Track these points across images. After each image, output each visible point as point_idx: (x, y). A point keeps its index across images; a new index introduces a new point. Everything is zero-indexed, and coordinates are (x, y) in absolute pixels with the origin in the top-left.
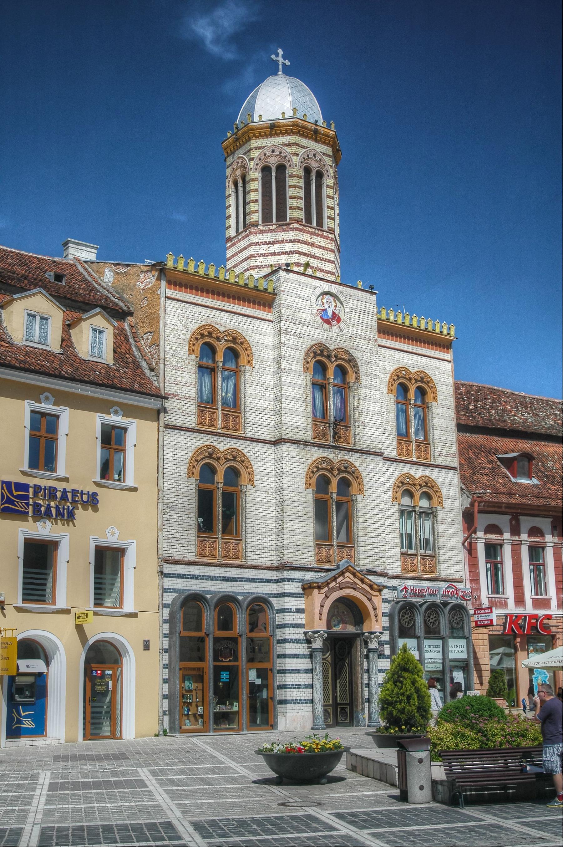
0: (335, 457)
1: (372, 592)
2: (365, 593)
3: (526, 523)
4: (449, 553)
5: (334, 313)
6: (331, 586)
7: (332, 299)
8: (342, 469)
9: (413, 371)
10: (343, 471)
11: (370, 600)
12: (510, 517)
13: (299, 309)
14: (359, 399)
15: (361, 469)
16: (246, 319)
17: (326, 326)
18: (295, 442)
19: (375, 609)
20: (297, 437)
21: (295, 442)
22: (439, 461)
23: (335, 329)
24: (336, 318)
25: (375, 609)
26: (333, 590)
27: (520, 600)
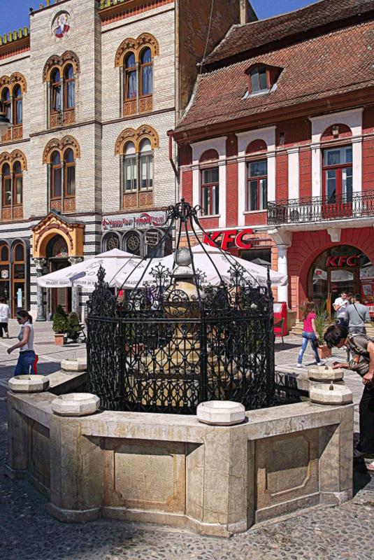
0: (59, 136)
1: (68, 229)
2: (64, 230)
3: (244, 139)
4: (162, 186)
5: (65, 26)
6: (42, 228)
7: (64, 15)
8: (65, 143)
9: (135, 38)
10: (67, 144)
11: (67, 234)
12: (225, 138)
13: (41, 37)
14: (79, 86)
15: (78, 139)
16: (23, 61)
17: (58, 39)
18: (37, 134)
19: (71, 241)
20: (39, 131)
21: (37, 134)
22: (156, 109)
23: (63, 38)
24: (67, 28)
25: (71, 241)
26: (44, 230)
27: (232, 216)
